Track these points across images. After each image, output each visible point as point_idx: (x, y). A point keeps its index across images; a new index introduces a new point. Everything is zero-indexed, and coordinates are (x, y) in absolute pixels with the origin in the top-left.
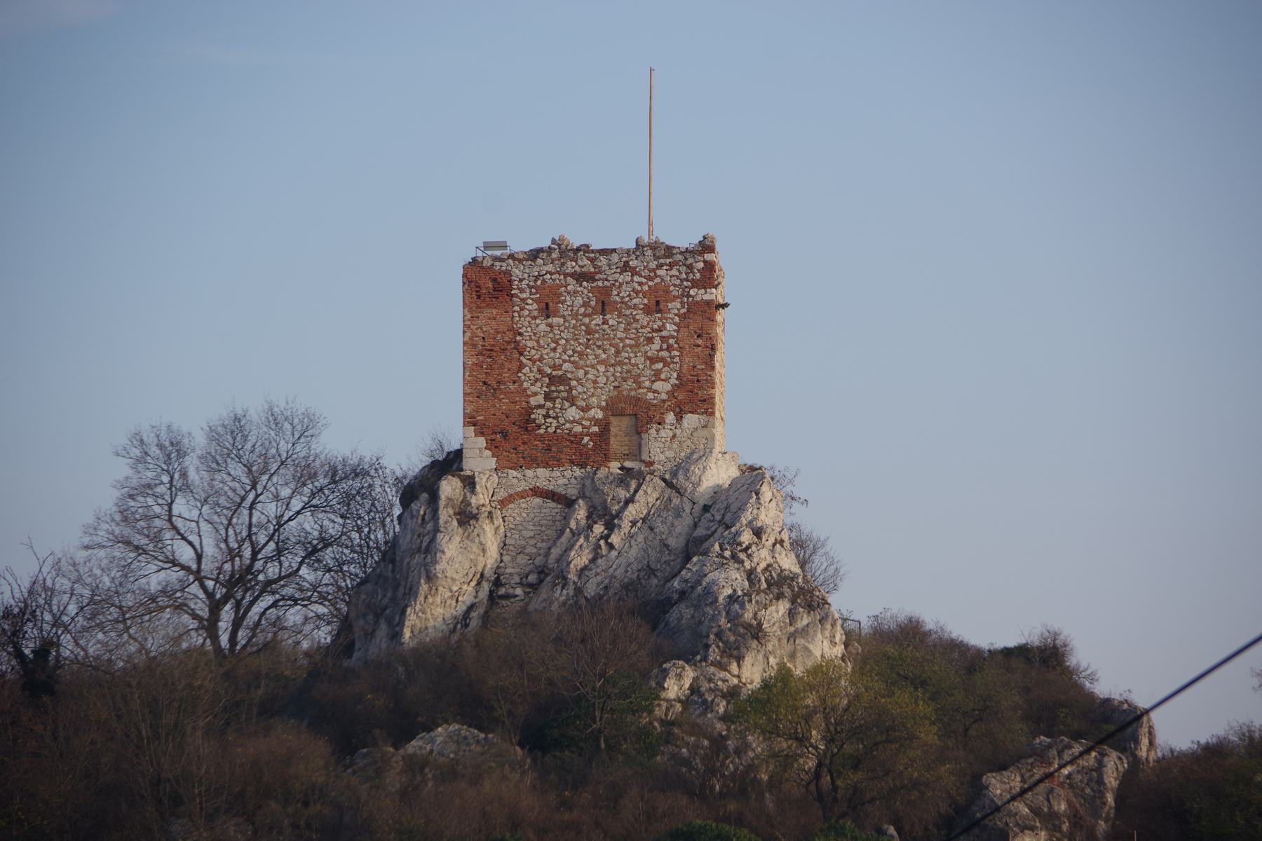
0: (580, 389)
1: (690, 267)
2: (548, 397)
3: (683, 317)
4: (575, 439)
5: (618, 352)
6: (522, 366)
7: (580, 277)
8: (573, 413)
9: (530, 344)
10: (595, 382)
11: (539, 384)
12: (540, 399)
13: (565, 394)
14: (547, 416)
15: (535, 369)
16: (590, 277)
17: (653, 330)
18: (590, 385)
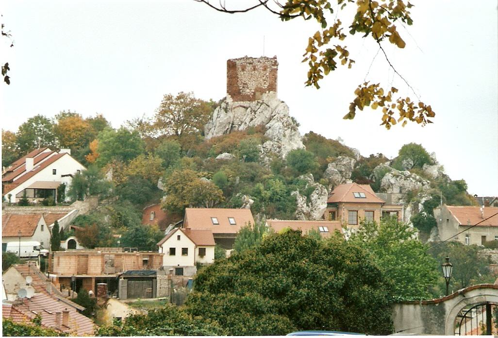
2: (243, 87)
3: (270, 72)
4: (248, 96)
7: (250, 63)
8: (248, 91)
12: (241, 88)
16: (251, 64)
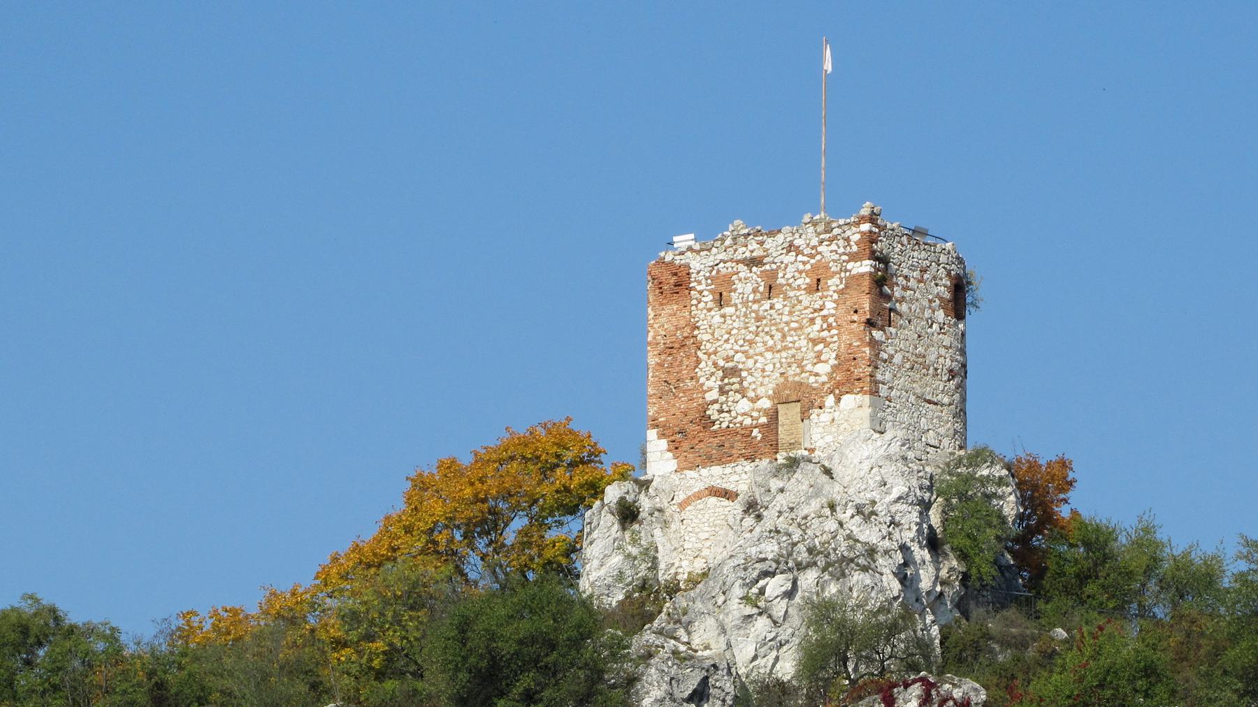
0: (750, 379)
1: (847, 240)
2: (722, 391)
5: (784, 336)
6: (698, 362)
9: (706, 337)
10: (763, 370)
11: (713, 378)
12: (714, 395)
13: (737, 386)
14: (721, 411)
15: (710, 363)
17: (815, 311)
18: (758, 374)
